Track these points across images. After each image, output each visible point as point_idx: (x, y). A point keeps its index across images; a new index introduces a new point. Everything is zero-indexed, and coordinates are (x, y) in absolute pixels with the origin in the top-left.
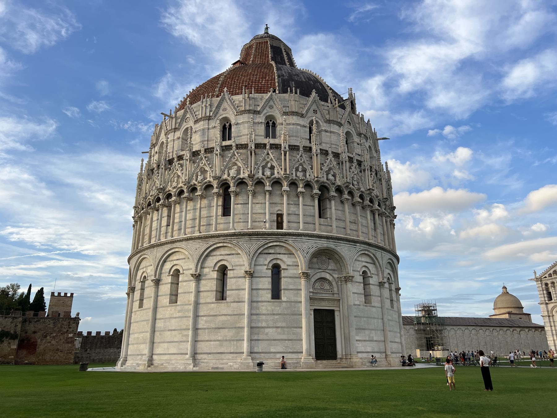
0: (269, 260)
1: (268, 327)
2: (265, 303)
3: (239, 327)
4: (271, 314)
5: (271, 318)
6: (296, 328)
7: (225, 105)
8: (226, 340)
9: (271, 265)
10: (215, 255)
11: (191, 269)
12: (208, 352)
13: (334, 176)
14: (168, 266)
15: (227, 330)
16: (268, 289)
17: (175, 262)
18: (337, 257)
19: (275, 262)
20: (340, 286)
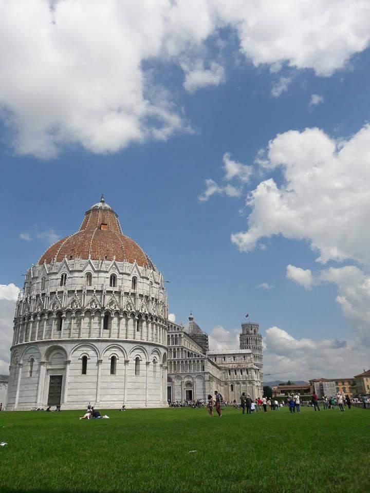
17: (114, 352)
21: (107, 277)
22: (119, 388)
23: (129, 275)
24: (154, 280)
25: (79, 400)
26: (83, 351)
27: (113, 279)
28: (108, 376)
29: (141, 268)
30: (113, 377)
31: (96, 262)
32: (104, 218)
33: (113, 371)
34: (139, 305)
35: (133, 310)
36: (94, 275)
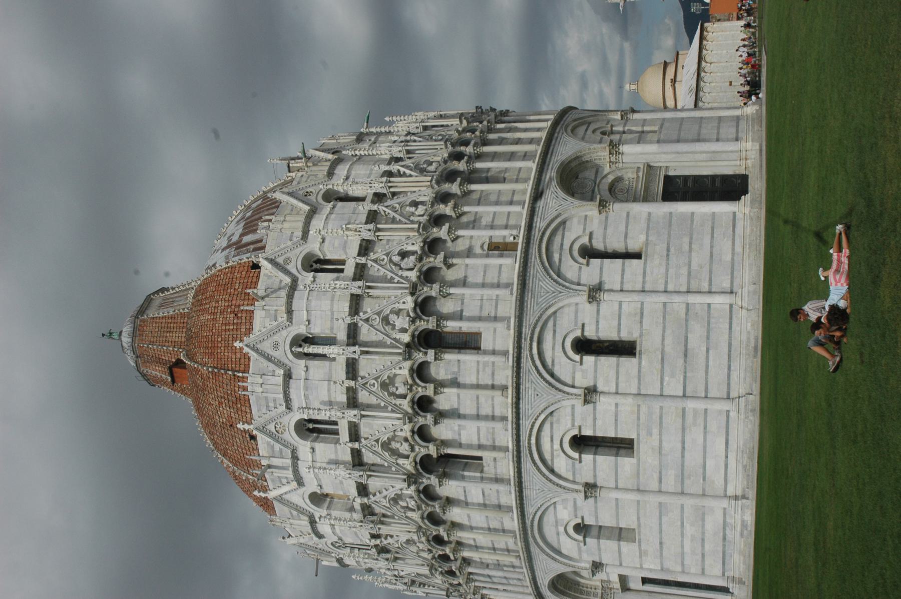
0: (572, 262)
1: (690, 265)
2: (648, 271)
3: (687, 314)
4: (668, 259)
5: (673, 259)
6: (692, 221)
7: (266, 347)
8: (708, 338)
9: (581, 260)
10: (553, 361)
11: (573, 407)
12: (726, 370)
13: (431, 163)
14: (561, 464)
15: (690, 336)
16: (623, 264)
17: (557, 446)
18: (573, 165)
19: (576, 253)
20: (625, 165)
21: (309, 450)
22: (683, 430)
23: (288, 376)
24: (296, 245)
25: (720, 549)
26: (558, 534)
27: (311, 429)
28: (638, 465)
29: (261, 320)
30: (644, 448)
31: (273, 480)
32: (159, 361)
33: (621, 446)
34: (386, 365)
35: (405, 372)
36: (312, 486)
